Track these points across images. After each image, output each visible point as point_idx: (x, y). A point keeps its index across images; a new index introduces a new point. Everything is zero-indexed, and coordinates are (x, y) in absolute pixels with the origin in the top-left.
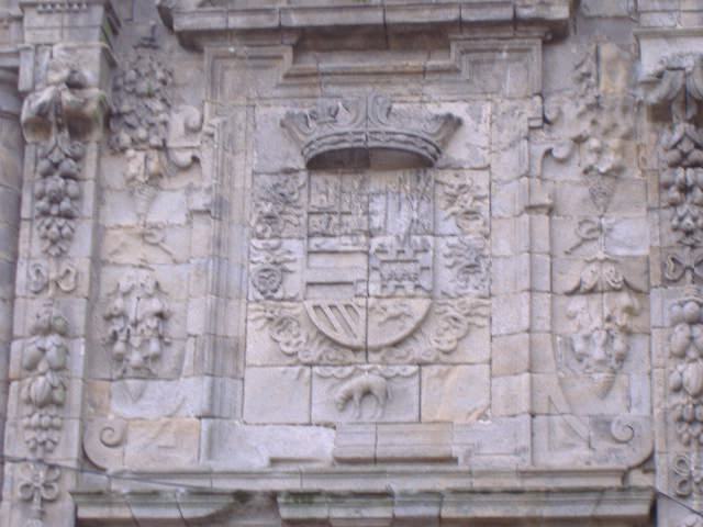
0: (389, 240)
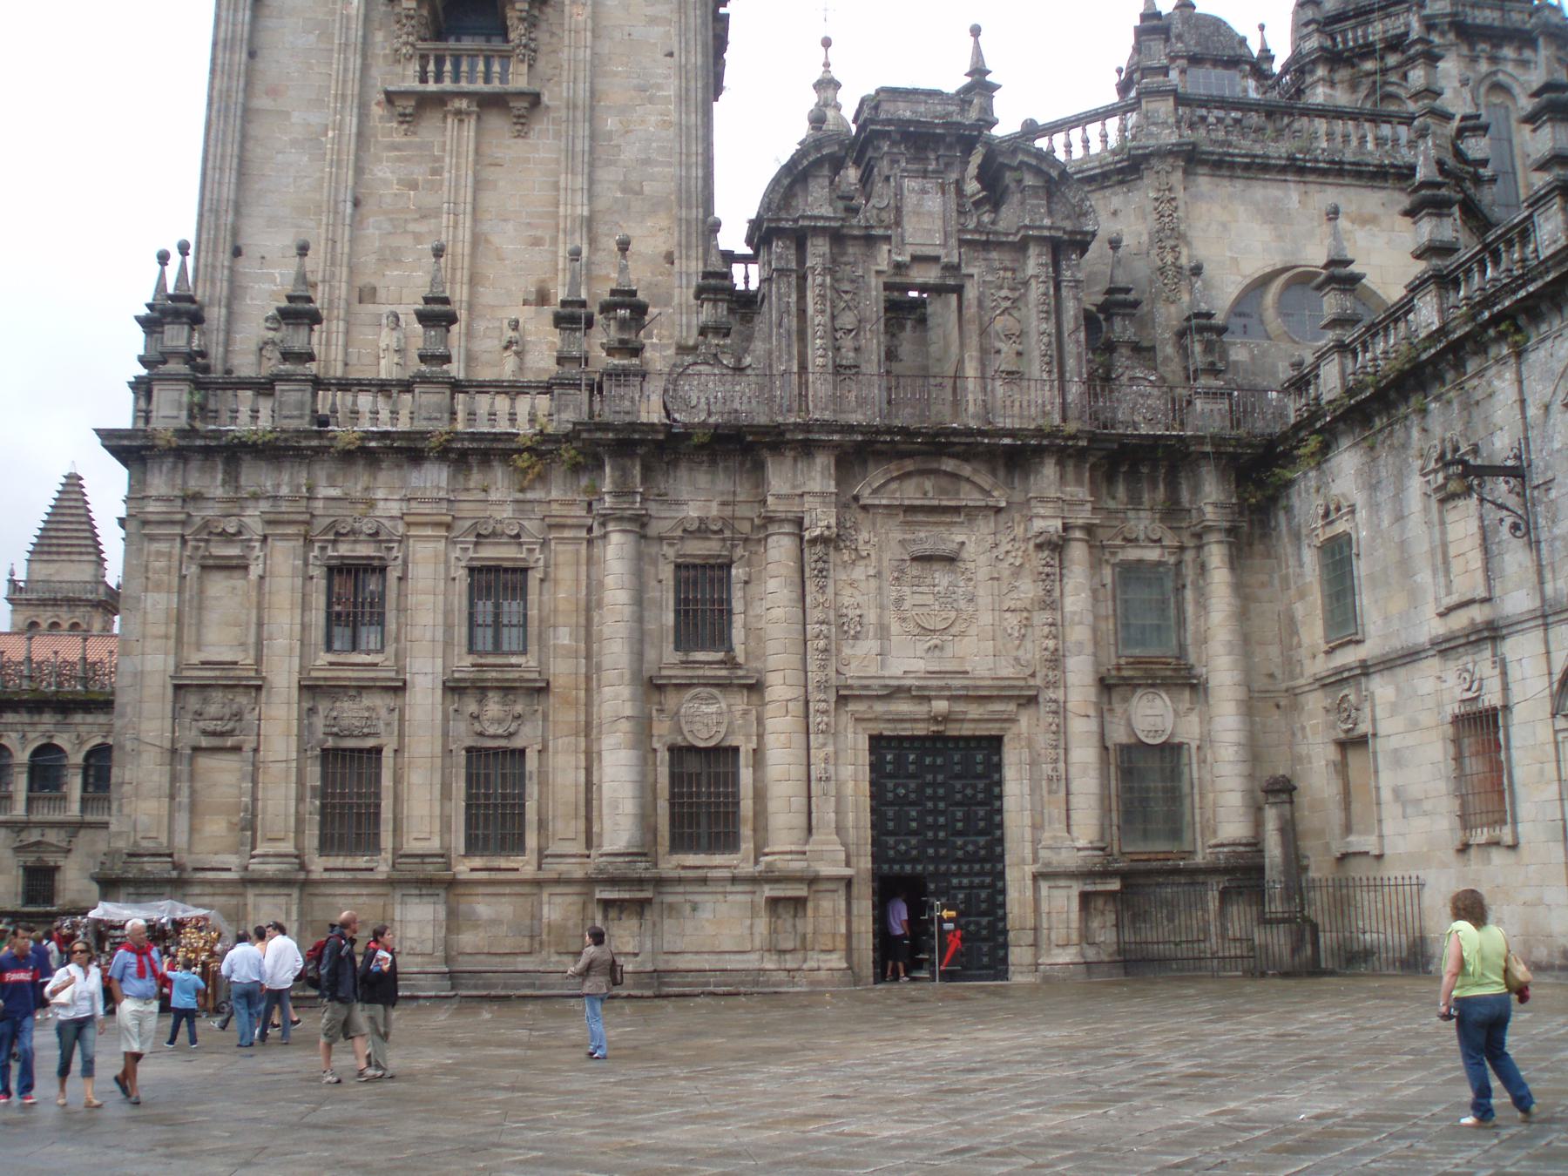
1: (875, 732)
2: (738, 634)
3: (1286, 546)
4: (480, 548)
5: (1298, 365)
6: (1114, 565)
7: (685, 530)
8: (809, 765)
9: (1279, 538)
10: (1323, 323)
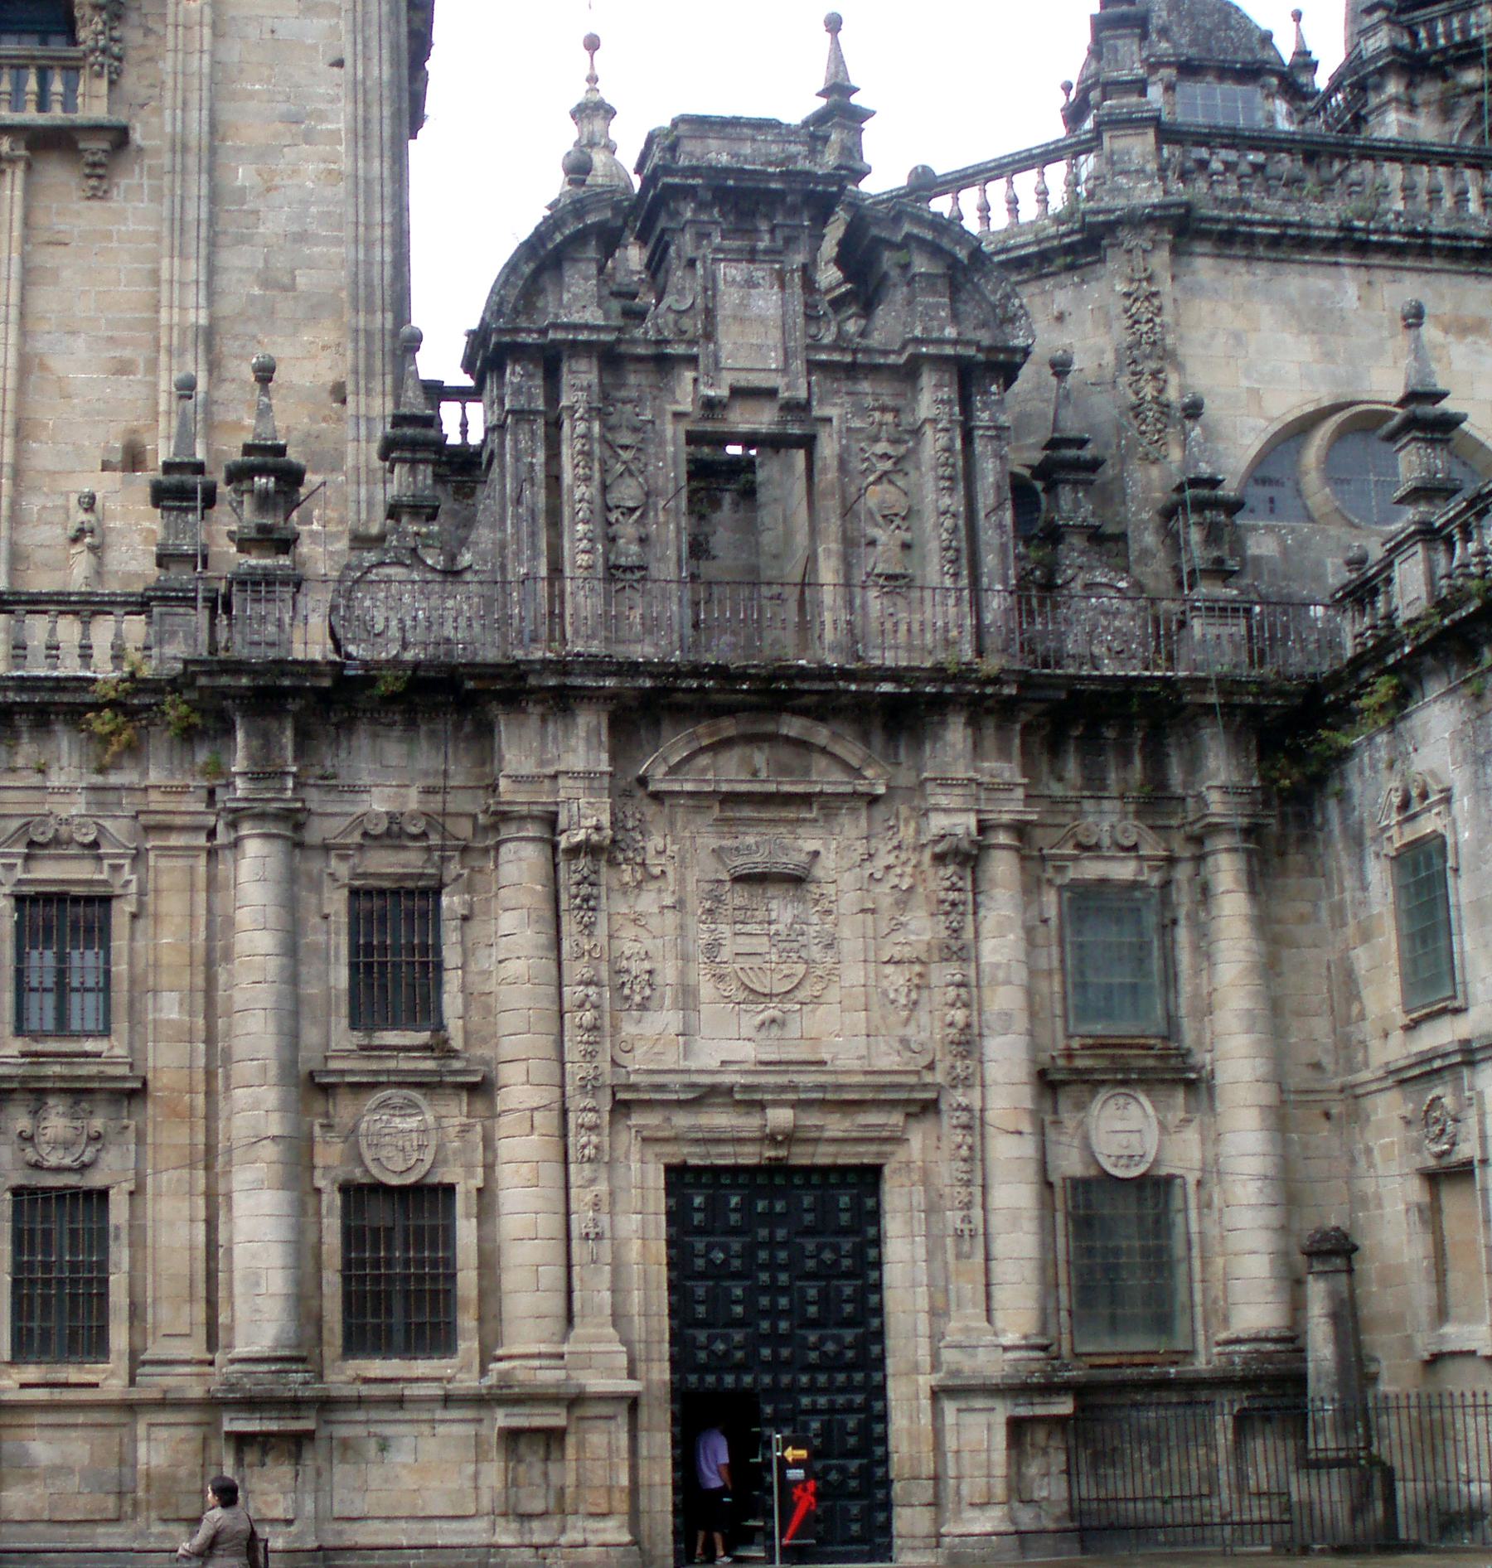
0: (780, 927)
1: (675, 1161)
2: (452, 1002)
3: (1340, 856)
4: (33, 864)
5: (1357, 563)
6: (1061, 889)
7: (365, 834)
8: (568, 1214)
9: (1328, 843)
10: (1398, 494)
